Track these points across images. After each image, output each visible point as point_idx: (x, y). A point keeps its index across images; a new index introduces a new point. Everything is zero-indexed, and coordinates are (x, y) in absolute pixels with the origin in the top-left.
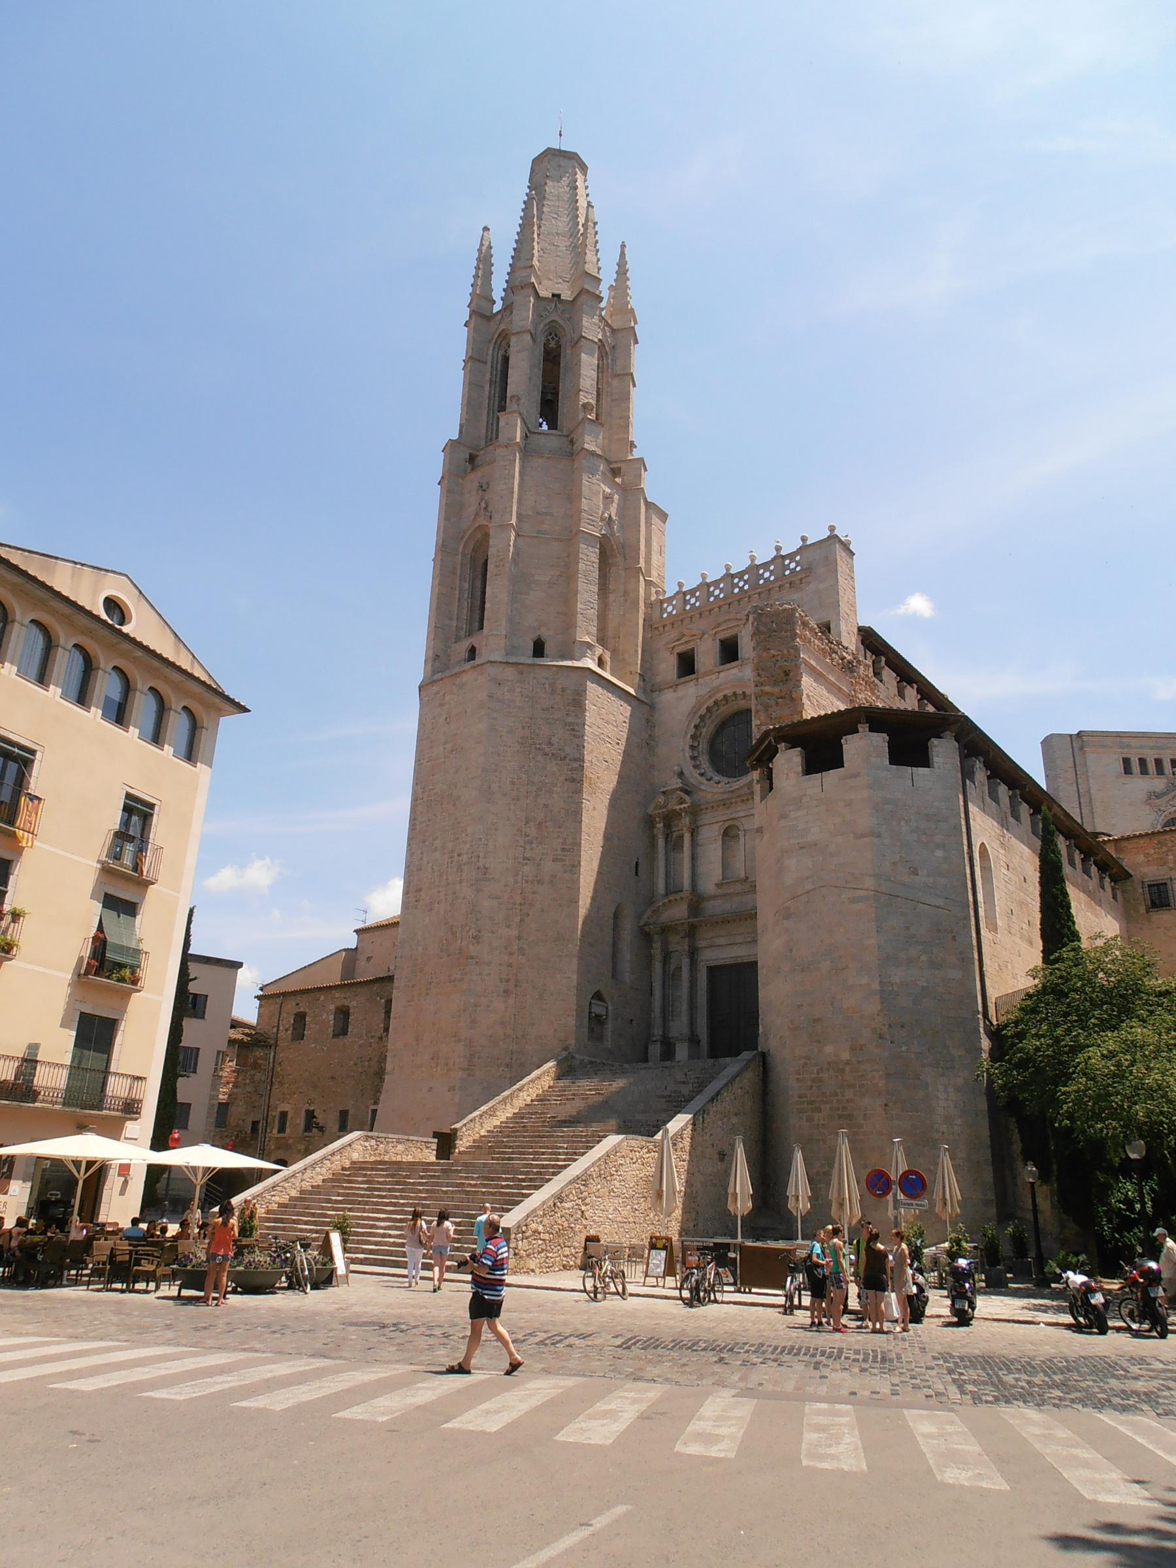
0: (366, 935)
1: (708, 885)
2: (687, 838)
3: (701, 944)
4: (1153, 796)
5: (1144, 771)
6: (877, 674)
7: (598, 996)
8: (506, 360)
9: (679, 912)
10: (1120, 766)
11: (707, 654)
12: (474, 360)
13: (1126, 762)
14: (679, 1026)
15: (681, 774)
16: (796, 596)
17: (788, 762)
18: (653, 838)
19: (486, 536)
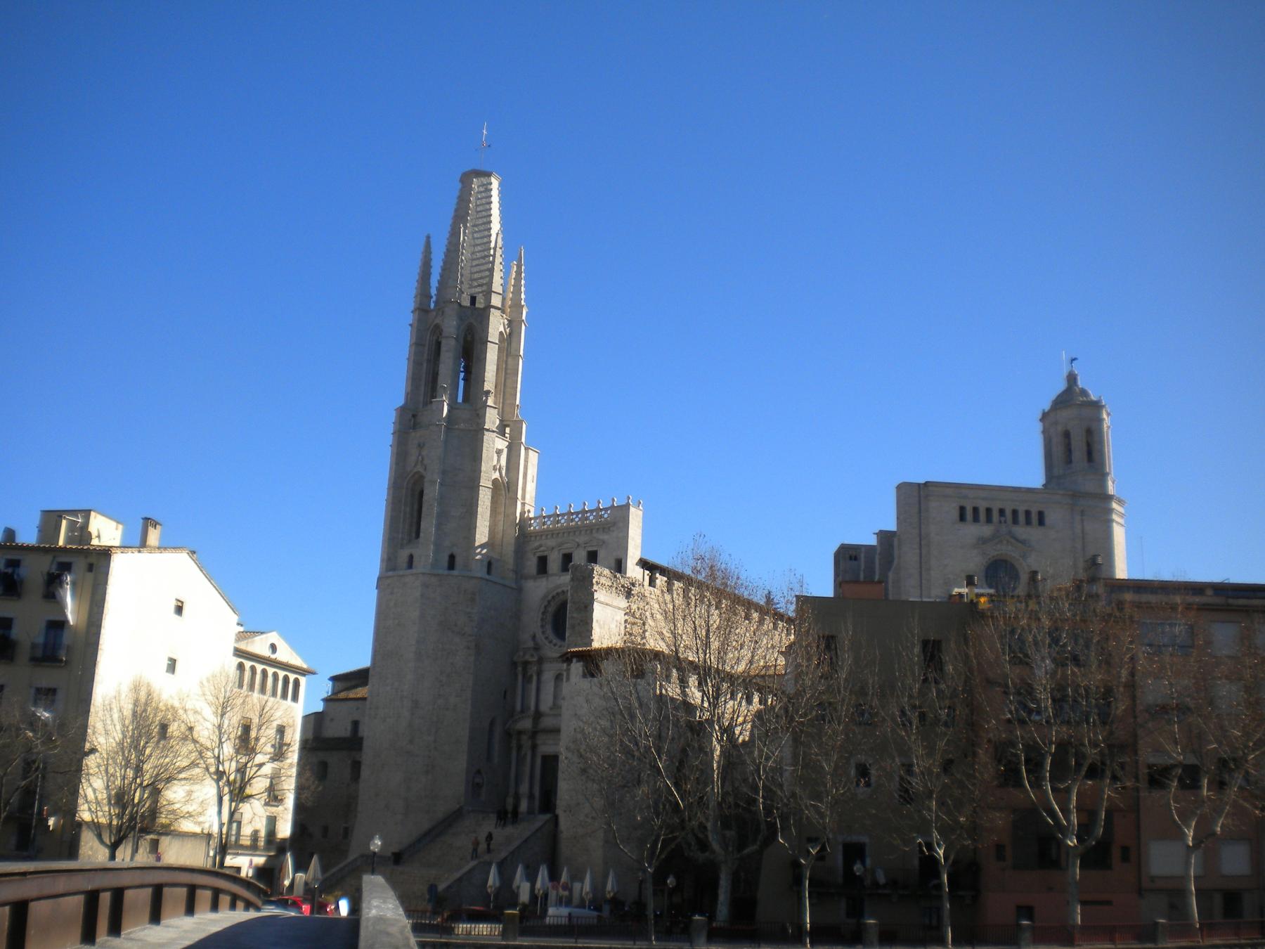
0: (331, 704)
1: (545, 706)
2: (535, 678)
3: (539, 742)
4: (983, 541)
5: (976, 519)
6: (652, 582)
7: (479, 772)
8: (439, 344)
9: (526, 724)
10: (956, 514)
11: (554, 563)
12: (418, 344)
13: (962, 509)
14: (524, 789)
15: (534, 637)
16: (605, 537)
17: (577, 667)
18: (516, 675)
19: (422, 477)
